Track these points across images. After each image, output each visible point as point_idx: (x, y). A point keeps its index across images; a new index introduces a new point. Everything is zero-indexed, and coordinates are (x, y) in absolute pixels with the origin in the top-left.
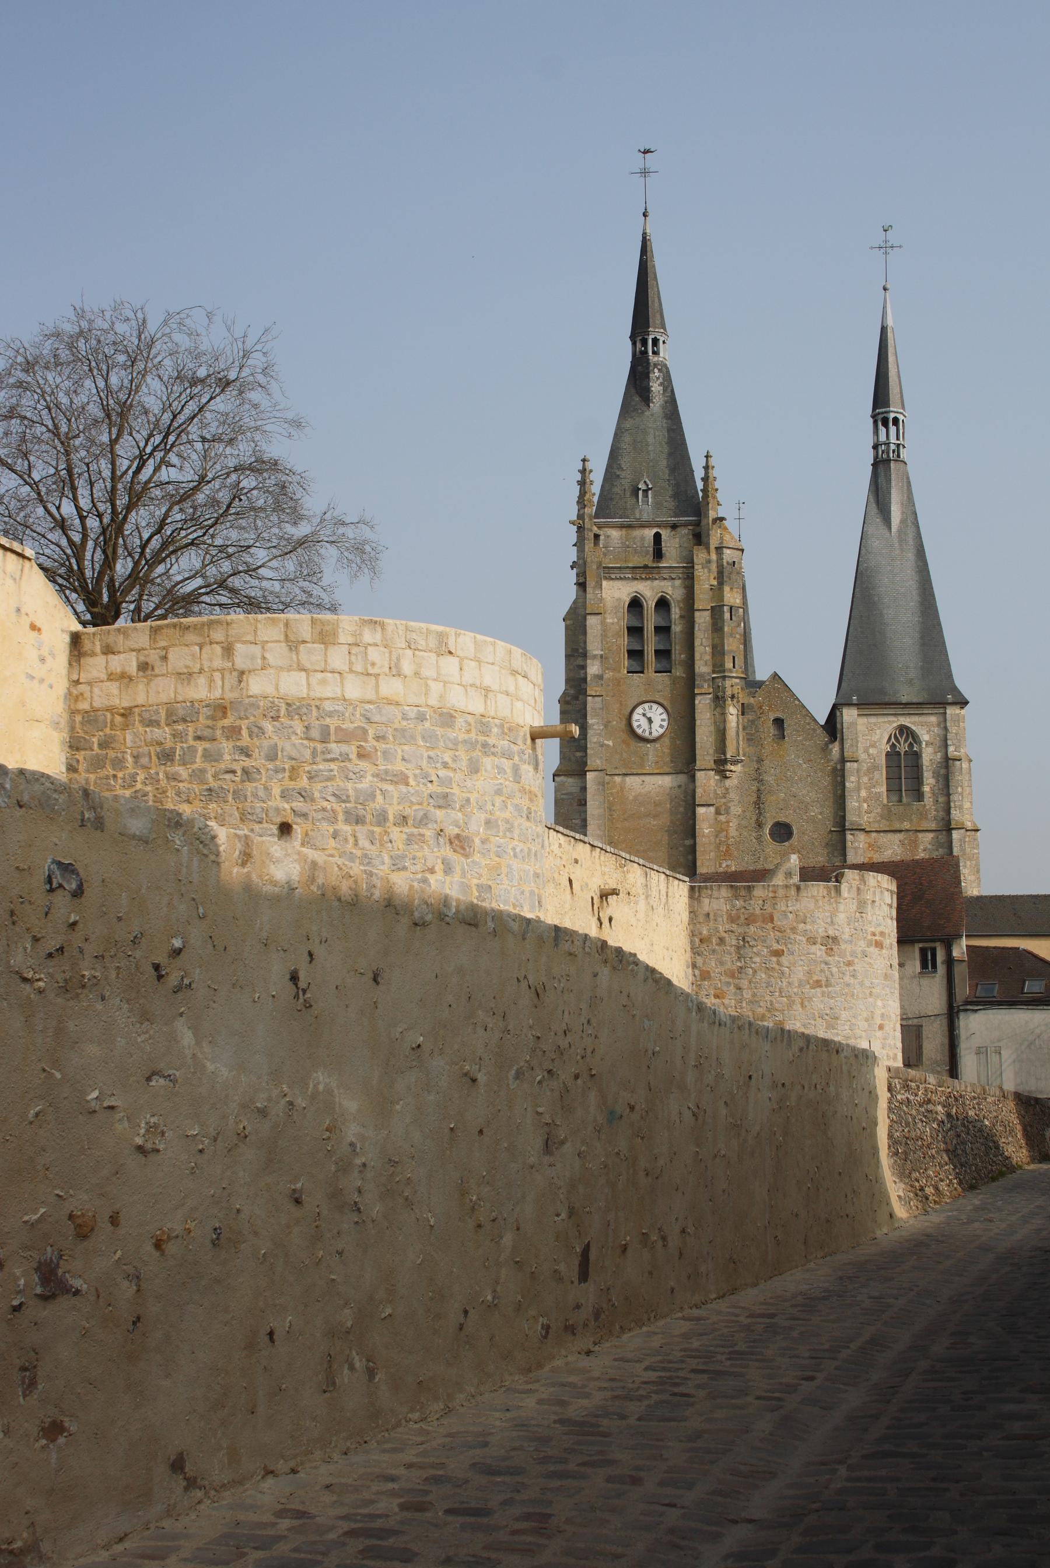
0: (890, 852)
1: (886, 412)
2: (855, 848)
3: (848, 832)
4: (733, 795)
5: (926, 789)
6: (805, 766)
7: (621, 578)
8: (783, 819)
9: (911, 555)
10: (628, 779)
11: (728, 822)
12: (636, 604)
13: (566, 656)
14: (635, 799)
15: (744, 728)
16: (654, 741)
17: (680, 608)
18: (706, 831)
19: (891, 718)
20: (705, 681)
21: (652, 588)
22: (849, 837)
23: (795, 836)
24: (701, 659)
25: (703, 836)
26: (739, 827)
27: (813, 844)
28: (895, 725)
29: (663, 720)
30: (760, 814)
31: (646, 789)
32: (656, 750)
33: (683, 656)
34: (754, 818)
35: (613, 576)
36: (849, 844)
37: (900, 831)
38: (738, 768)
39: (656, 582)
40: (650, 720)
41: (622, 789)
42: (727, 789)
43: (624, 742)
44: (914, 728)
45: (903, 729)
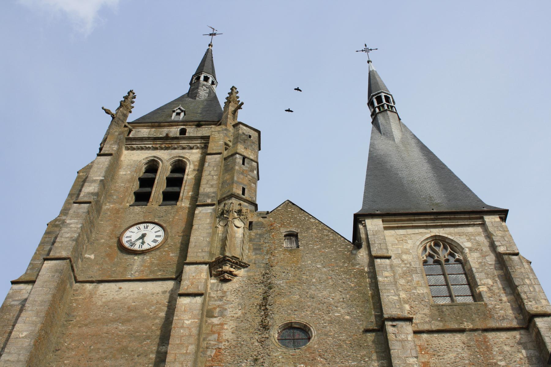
0: (452, 355)
1: (378, 93)
2: (402, 341)
3: (388, 324)
4: (230, 297)
5: (482, 289)
6: (325, 270)
7: (142, 149)
8: (296, 318)
10: (102, 286)
11: (222, 324)
12: (152, 167)
13: (69, 195)
14: (106, 304)
15: (251, 240)
17: (195, 165)
20: (209, 198)
24: (207, 183)
25: (182, 327)
26: (237, 330)
27: (340, 346)
29: (157, 236)
30: (266, 316)
31: (121, 296)
33: (190, 193)
34: (259, 319)
35: (134, 146)
36: (391, 337)
37: (462, 331)
38: (241, 272)
41: (92, 294)
42: (225, 292)
43: (108, 255)
44: (451, 238)
45: (438, 240)
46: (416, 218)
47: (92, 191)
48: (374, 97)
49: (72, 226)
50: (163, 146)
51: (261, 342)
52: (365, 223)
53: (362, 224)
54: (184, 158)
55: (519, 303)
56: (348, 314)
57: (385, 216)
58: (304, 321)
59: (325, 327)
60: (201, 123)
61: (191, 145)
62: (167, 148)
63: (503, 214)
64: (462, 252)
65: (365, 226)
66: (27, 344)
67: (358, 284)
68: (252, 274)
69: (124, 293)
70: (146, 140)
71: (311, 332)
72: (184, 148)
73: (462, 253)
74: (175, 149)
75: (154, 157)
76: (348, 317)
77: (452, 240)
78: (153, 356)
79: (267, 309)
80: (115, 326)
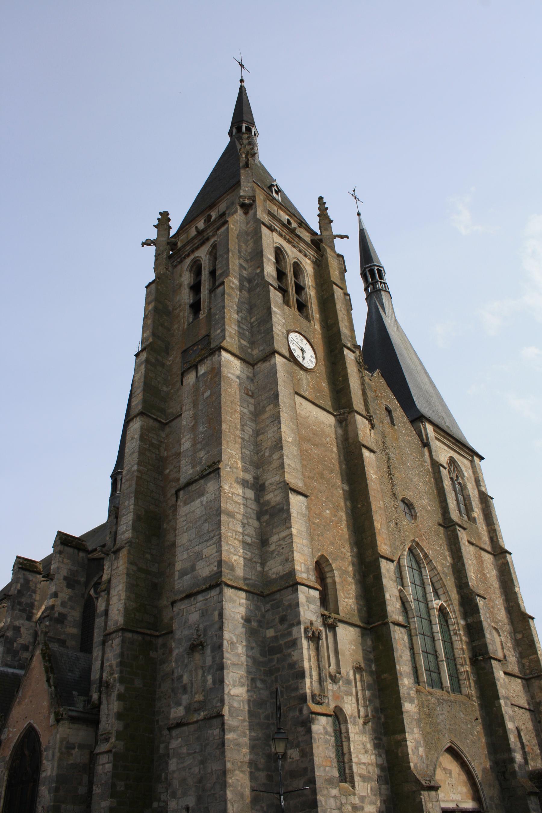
9: (412, 351)
16: (306, 370)
18: (374, 477)
19: (446, 448)
21: (292, 252)
22: (459, 533)
23: (419, 519)
25: (372, 480)
28: (449, 455)
32: (307, 379)
34: (390, 486)
39: (294, 250)
40: (302, 350)
46: (447, 437)
47: (272, 273)
48: (376, 268)
49: (278, 316)
50: (288, 237)
51: (396, 508)
52: (425, 425)
53: (423, 425)
54: (301, 263)
55: (491, 535)
56: (429, 505)
57: (437, 427)
58: (412, 500)
59: (421, 510)
60: (303, 225)
61: (308, 254)
62: (289, 242)
63: (481, 458)
64: (463, 476)
65: (425, 428)
66: (296, 453)
67: (430, 481)
68: (377, 438)
69: (305, 411)
70: (276, 220)
71: (415, 511)
72: (300, 251)
73: (462, 479)
74: (294, 247)
75: (281, 245)
76: (429, 508)
77: (459, 466)
78: (340, 491)
79: (391, 479)
80: (310, 446)
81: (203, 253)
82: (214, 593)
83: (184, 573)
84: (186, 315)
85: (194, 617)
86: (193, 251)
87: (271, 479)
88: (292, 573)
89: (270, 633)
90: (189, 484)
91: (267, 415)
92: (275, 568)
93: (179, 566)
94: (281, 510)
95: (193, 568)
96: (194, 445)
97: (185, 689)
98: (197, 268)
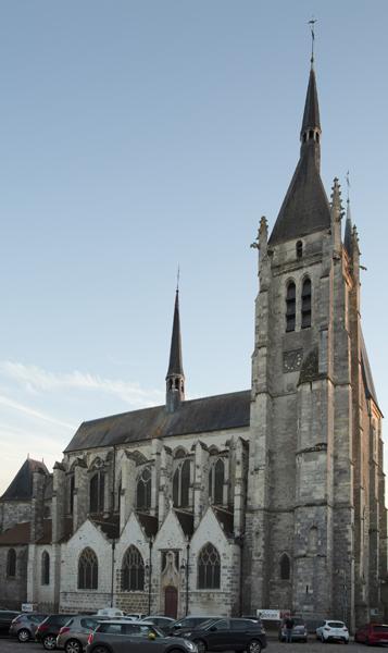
81: (297, 277)
82: (322, 508)
83: (304, 494)
84: (283, 322)
85: (311, 515)
86: (289, 271)
87: (342, 455)
88: (348, 502)
89: (336, 525)
90: (310, 450)
91: (341, 419)
92: (341, 498)
93: (302, 490)
94: (345, 472)
95: (310, 494)
96: (310, 429)
97: (306, 544)
98: (291, 286)
